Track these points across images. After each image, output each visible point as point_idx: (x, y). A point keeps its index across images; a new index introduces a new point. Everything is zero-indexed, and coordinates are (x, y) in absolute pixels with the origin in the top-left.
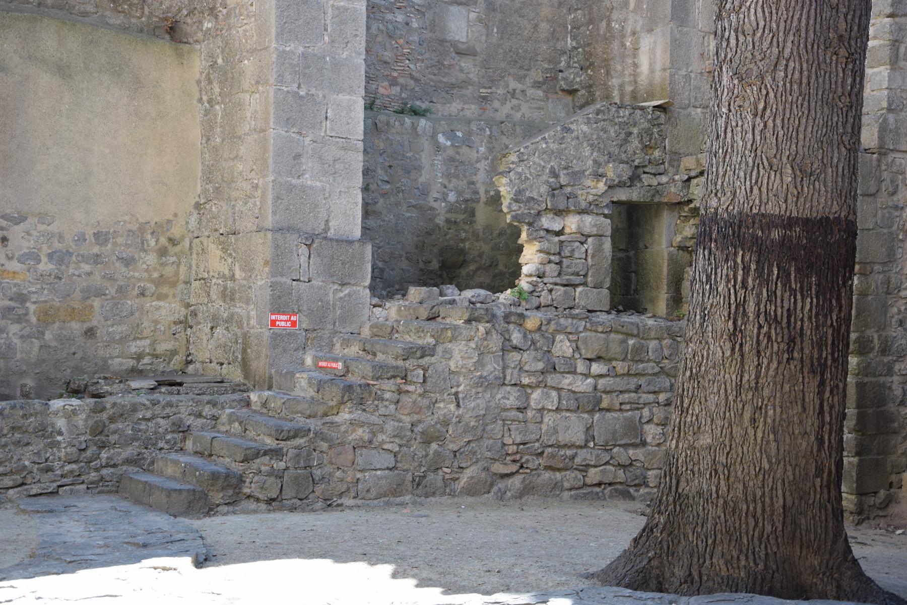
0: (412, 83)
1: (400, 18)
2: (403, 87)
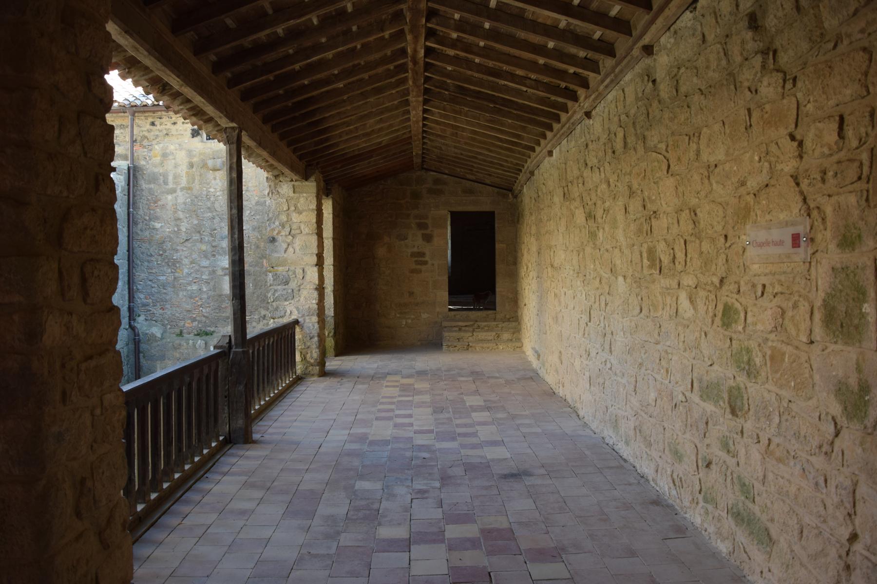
0: (204, 319)
1: (195, 287)
2: (199, 322)
